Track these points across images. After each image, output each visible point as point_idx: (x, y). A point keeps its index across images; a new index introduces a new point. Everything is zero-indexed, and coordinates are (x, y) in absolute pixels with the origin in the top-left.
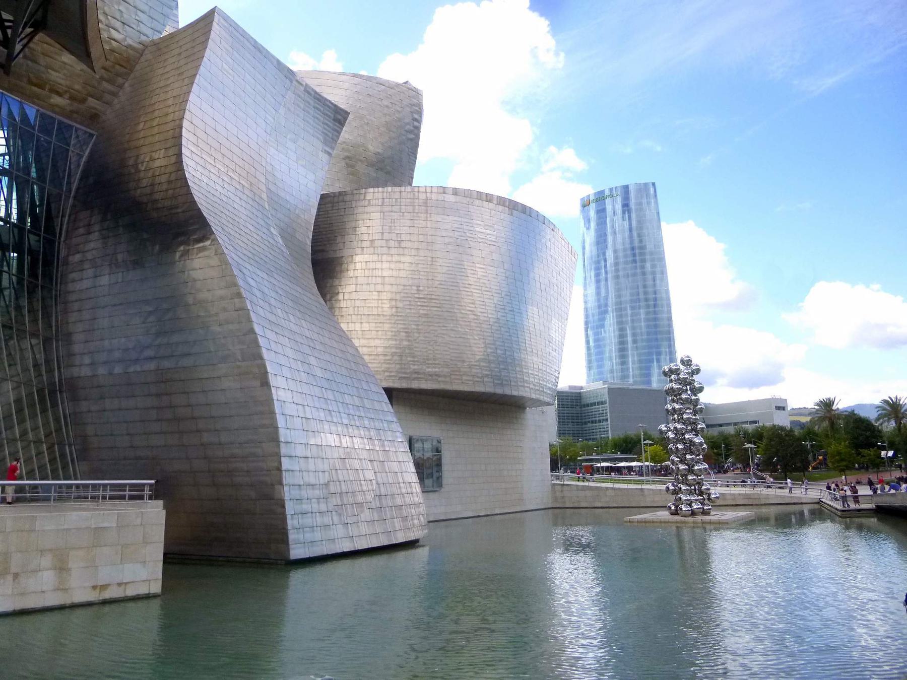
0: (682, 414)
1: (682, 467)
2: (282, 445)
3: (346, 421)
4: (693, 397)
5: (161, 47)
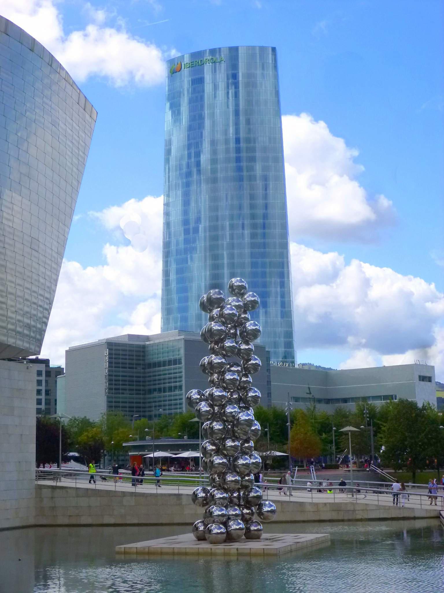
0: (223, 373)
1: (218, 460)
4: (244, 347)
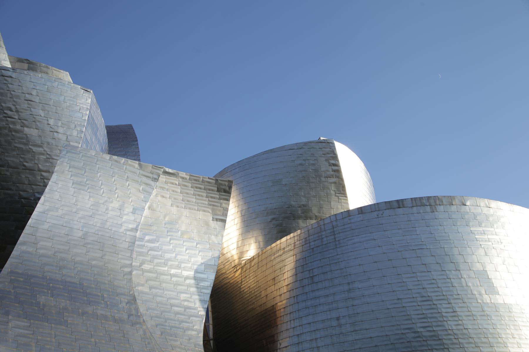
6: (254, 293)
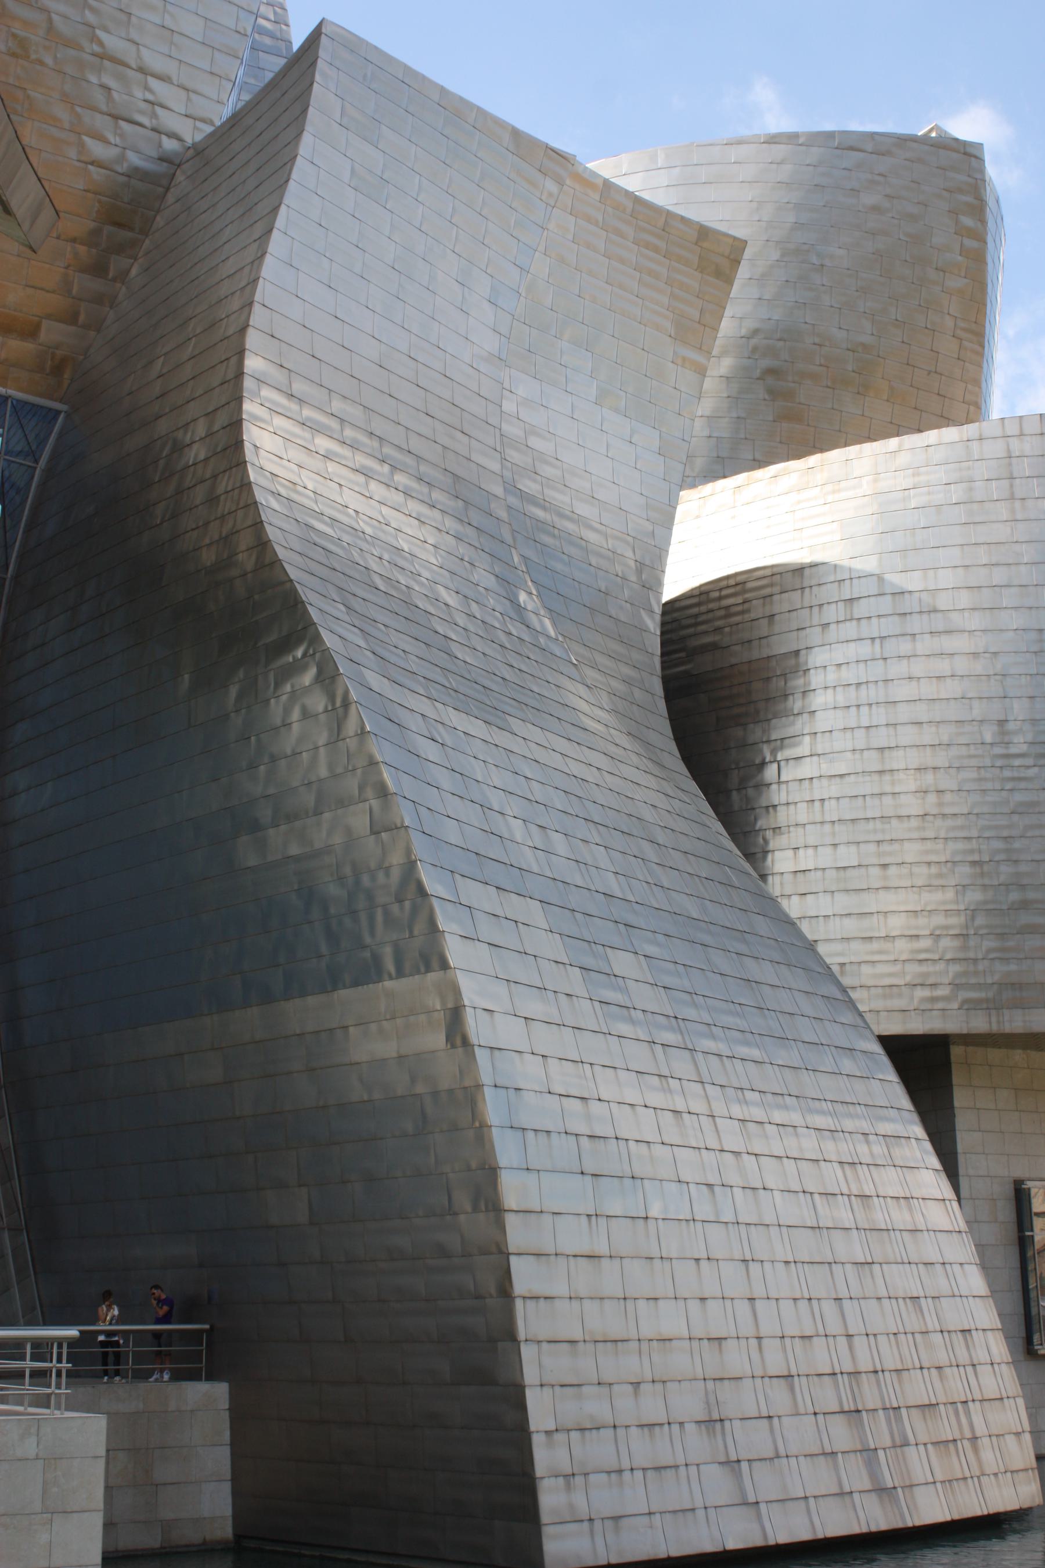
2: (510, 1220)
3: (733, 1142)
5: (207, 157)
6: (720, 598)
